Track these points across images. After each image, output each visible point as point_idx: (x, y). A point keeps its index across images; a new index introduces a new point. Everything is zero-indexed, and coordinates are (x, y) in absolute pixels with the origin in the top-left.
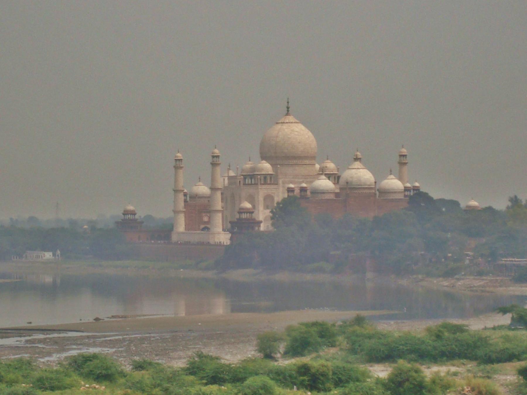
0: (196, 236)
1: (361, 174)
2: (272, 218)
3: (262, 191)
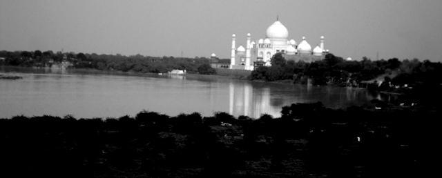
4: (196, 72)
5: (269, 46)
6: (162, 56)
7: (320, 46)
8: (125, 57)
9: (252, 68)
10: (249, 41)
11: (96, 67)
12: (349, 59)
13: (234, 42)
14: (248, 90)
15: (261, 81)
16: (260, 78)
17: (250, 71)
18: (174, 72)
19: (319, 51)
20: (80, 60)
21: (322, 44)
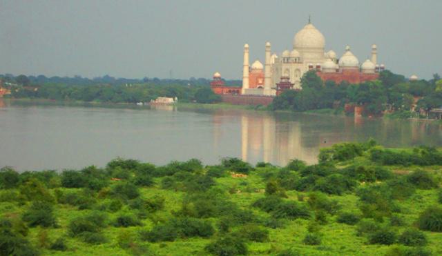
0: (256, 92)
1: (349, 60)
2: (301, 82)
3: (294, 67)
4: (193, 99)
5: (298, 61)
6: (141, 78)
7: (371, 60)
8: (86, 79)
9: (274, 93)
10: (268, 54)
11: (45, 95)
12: (414, 77)
13: (246, 56)
14: (268, 125)
15: (287, 111)
16: (286, 107)
17: (271, 96)
18: (160, 100)
19: (369, 65)
20: (22, 86)
21: (374, 57)
